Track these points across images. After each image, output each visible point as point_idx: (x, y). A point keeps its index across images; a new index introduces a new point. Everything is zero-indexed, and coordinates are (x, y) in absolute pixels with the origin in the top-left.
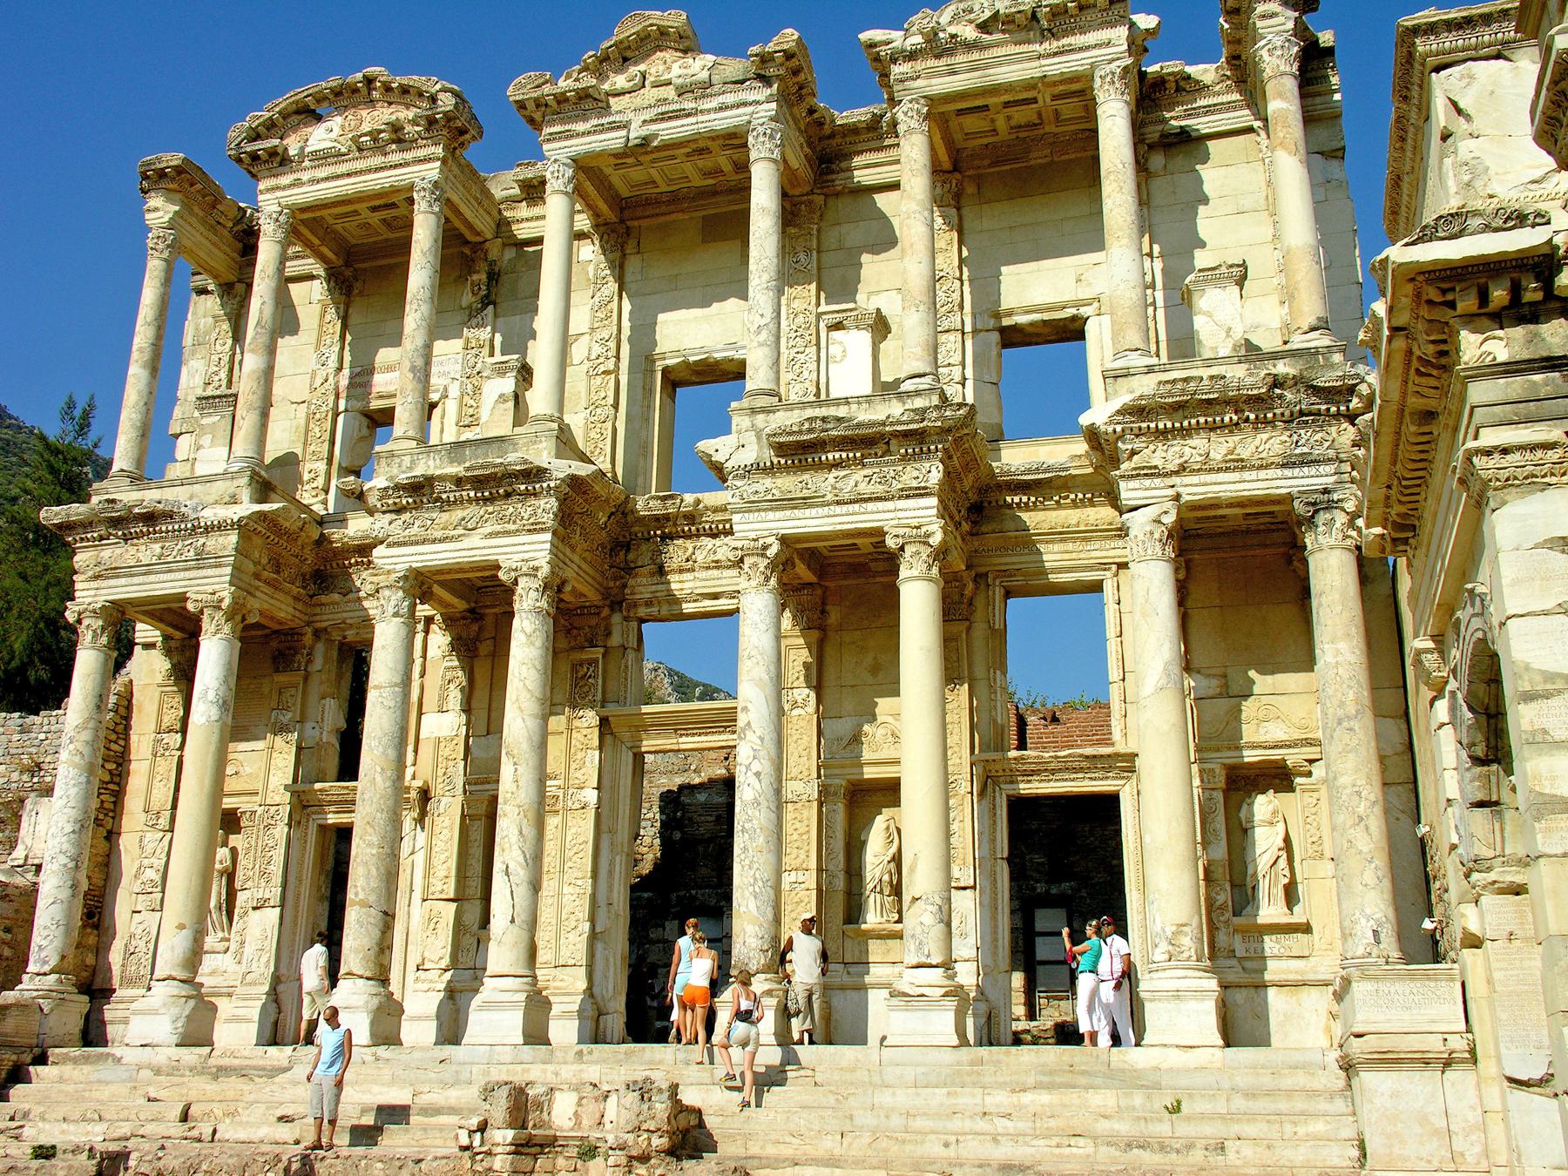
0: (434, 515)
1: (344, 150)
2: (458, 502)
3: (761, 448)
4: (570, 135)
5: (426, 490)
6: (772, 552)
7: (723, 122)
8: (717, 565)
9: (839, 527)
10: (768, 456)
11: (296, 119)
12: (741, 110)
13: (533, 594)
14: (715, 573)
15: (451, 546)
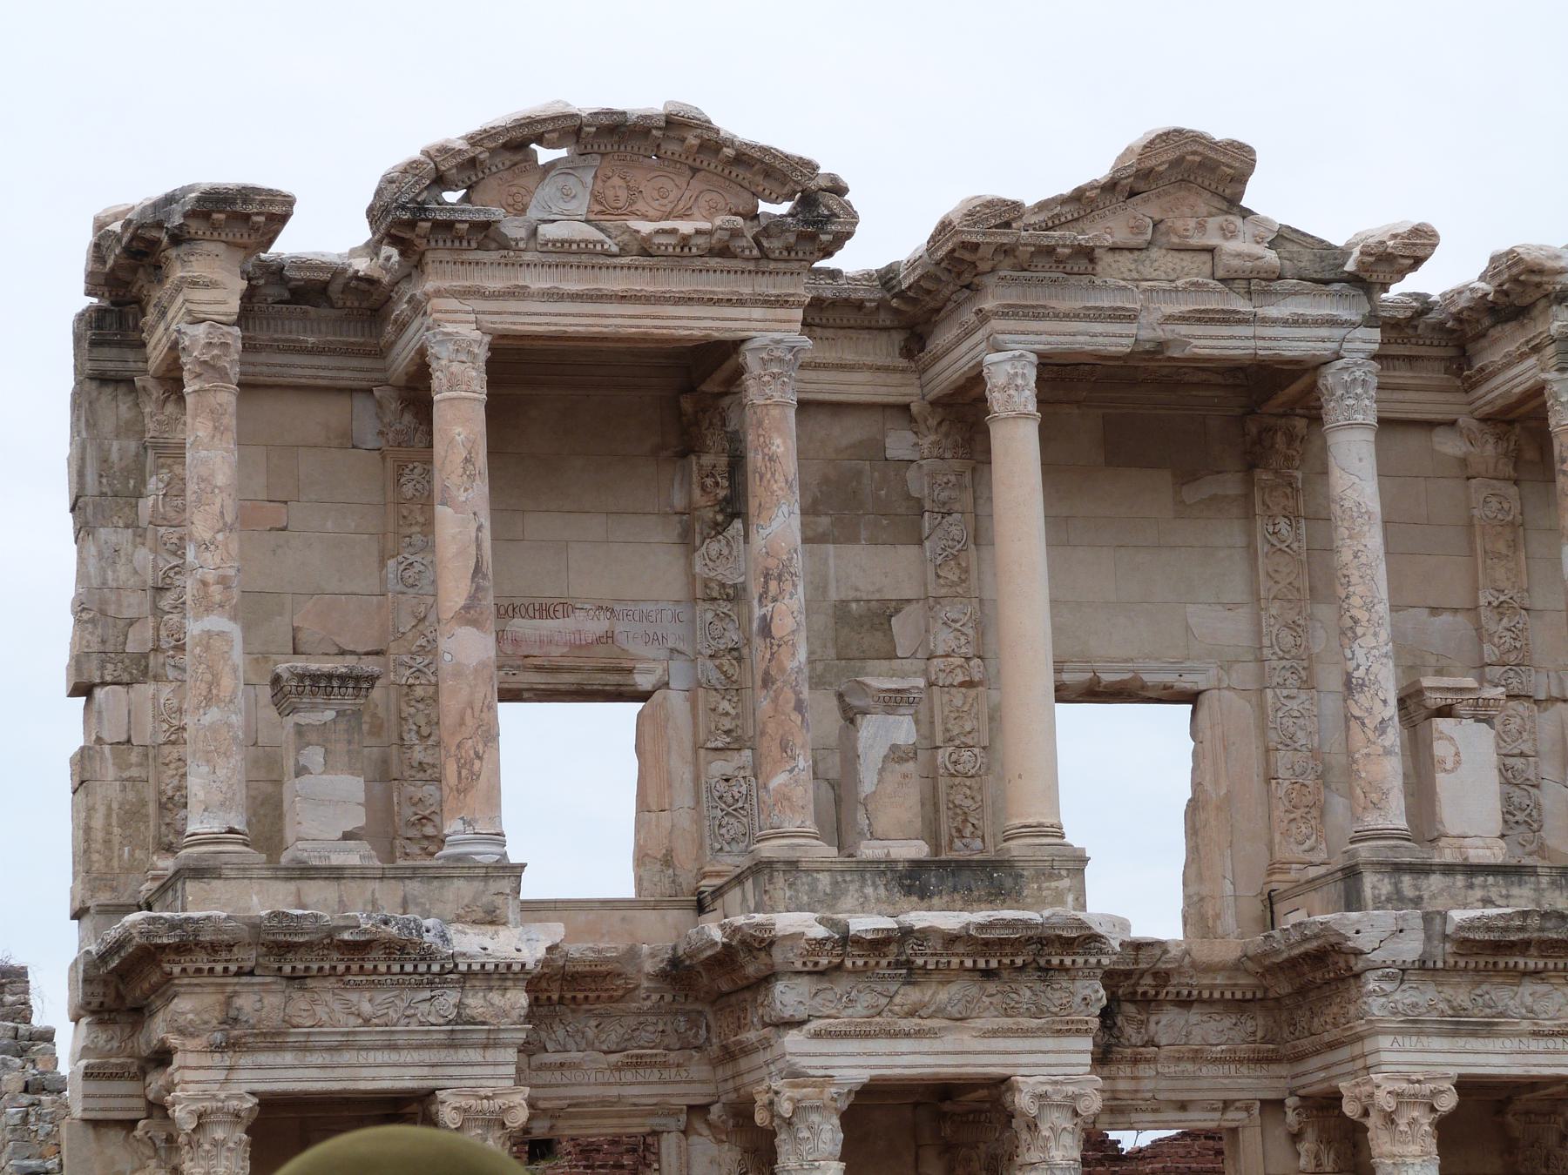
0: (893, 988)
1: (615, 249)
2: (945, 975)
3: (1428, 939)
4: (1038, 313)
5: (894, 948)
6: (1448, 1102)
7: (1295, 345)
8: (1196, 1057)
9: (1535, 1071)
10: (1443, 953)
11: (508, 158)
12: (1324, 332)
13: (1067, 1139)
14: (1190, 1067)
15: (925, 1045)
